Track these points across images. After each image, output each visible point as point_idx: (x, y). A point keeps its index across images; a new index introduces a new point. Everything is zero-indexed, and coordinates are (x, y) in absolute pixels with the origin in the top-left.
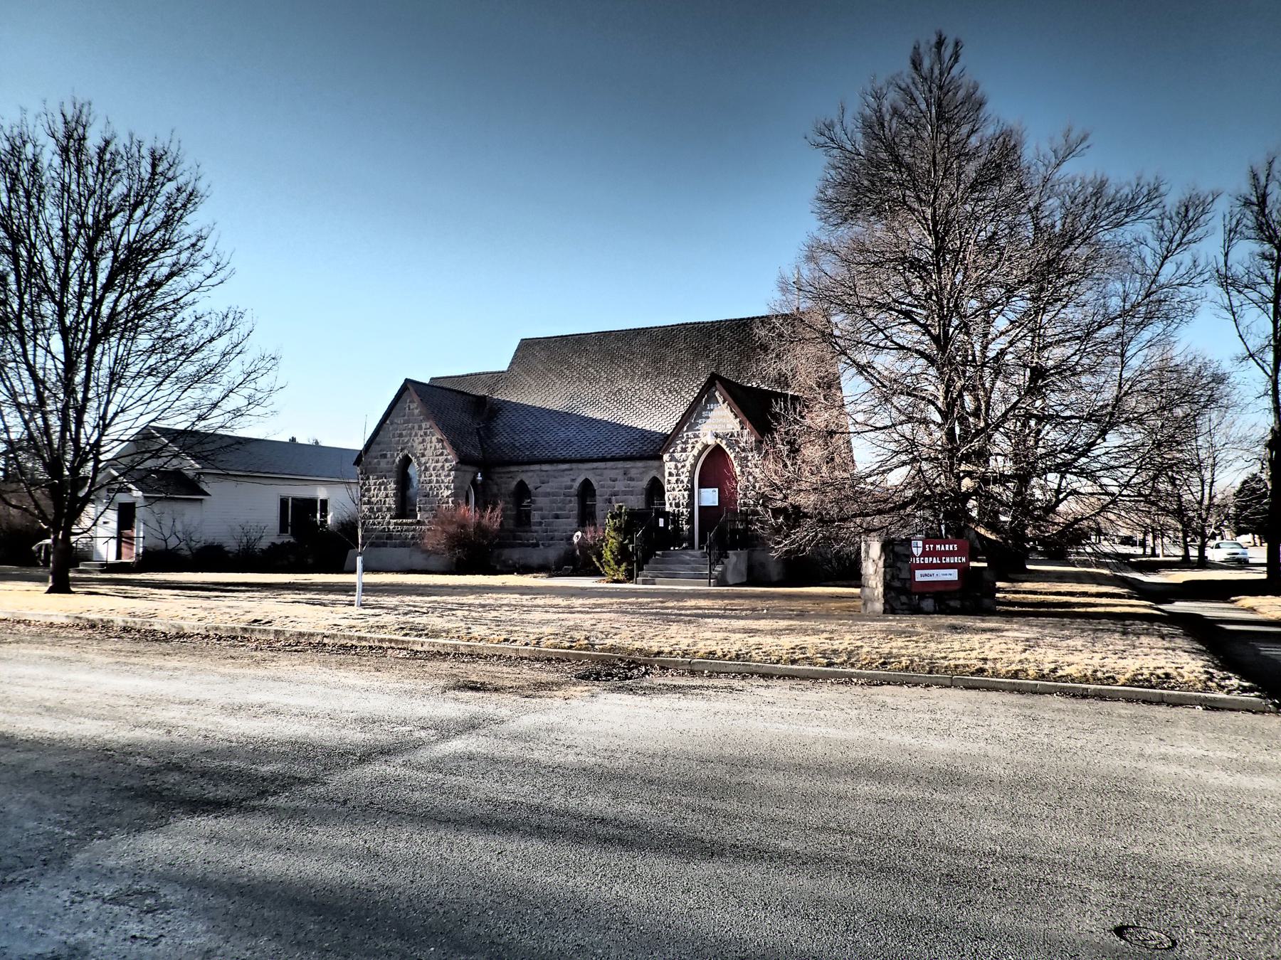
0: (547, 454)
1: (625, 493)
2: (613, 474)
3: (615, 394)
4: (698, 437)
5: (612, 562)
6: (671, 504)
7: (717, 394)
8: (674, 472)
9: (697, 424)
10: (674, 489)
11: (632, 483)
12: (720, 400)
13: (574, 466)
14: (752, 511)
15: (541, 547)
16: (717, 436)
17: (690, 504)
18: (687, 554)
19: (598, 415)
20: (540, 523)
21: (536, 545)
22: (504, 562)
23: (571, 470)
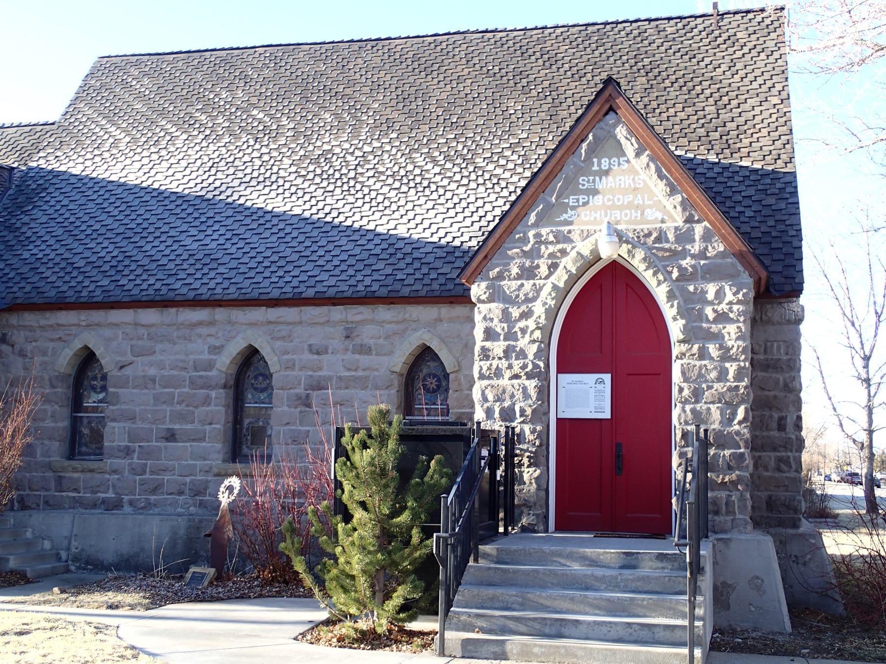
0: (151, 285)
1: (345, 383)
2: (317, 336)
3: (316, 161)
4: (568, 240)
5: (362, 583)
6: (489, 413)
7: (621, 132)
8: (499, 327)
9: (565, 208)
10: (498, 374)
11: (364, 360)
12: (629, 148)
13: (220, 314)
14: (719, 434)
15: (127, 509)
16: (621, 238)
17: (540, 414)
18: (570, 556)
19: (277, 204)
20: (127, 452)
21: (114, 506)
22: (29, 544)
23: (212, 323)
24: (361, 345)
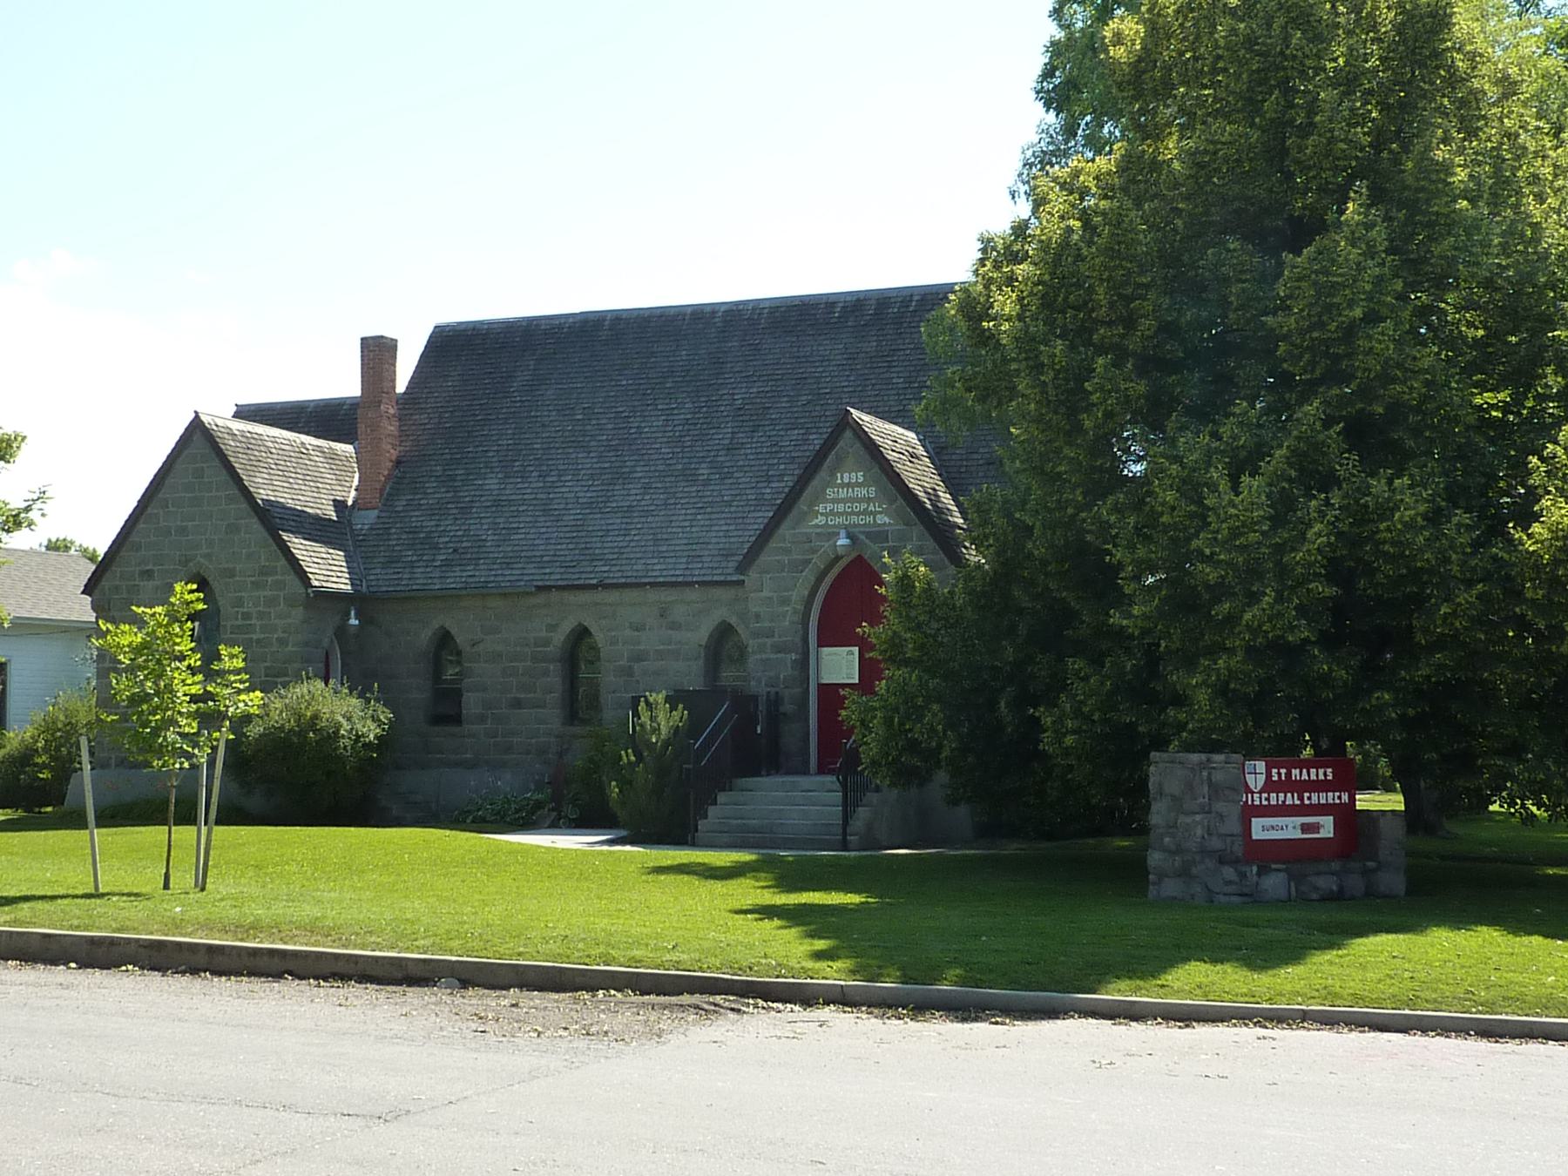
20: (482, 719)
24: (673, 622)
